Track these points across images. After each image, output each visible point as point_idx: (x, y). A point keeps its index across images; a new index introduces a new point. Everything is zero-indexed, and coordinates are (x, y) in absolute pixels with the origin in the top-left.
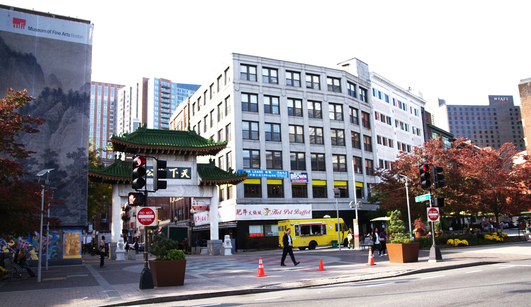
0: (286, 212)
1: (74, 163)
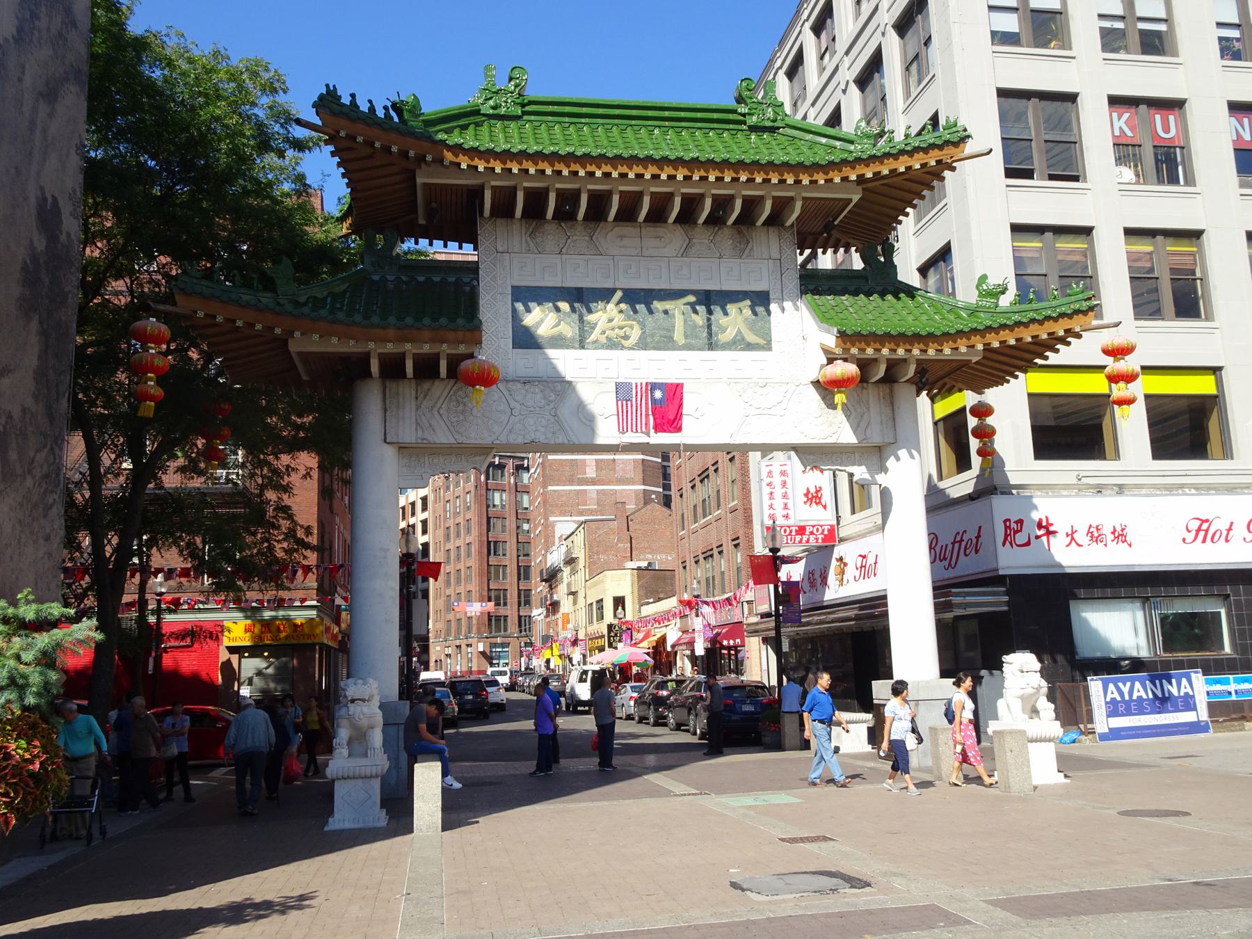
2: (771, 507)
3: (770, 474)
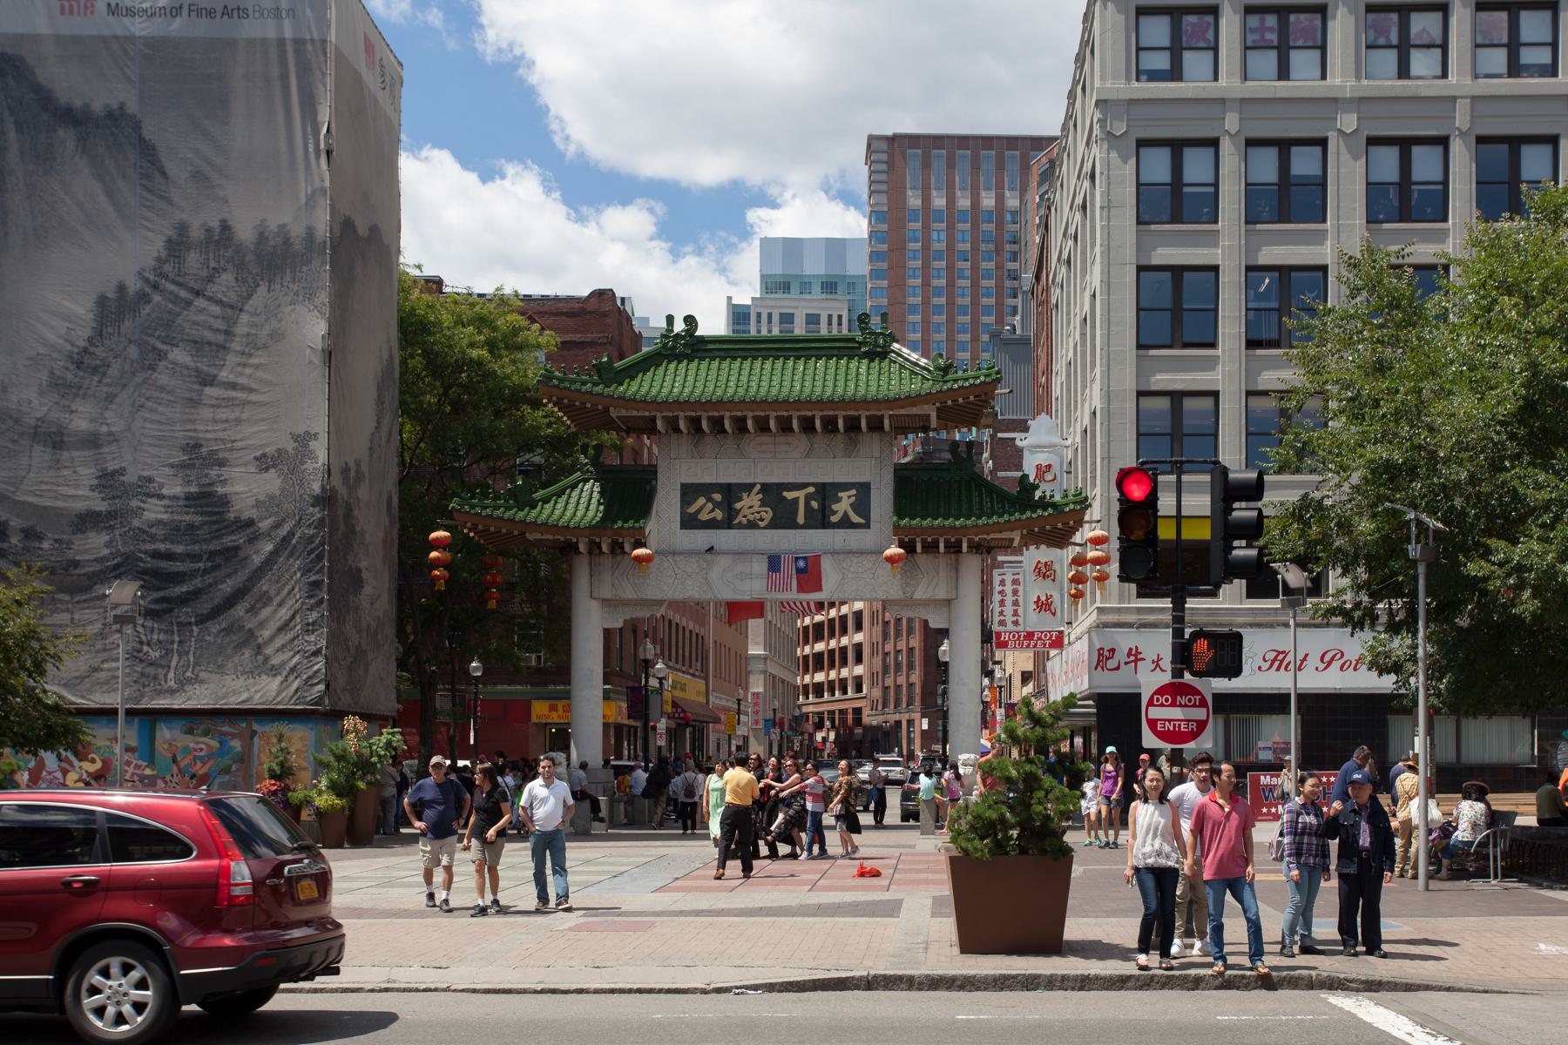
0: (1330, 663)
1: (283, 490)
2: (1001, 613)
3: (1002, 583)
